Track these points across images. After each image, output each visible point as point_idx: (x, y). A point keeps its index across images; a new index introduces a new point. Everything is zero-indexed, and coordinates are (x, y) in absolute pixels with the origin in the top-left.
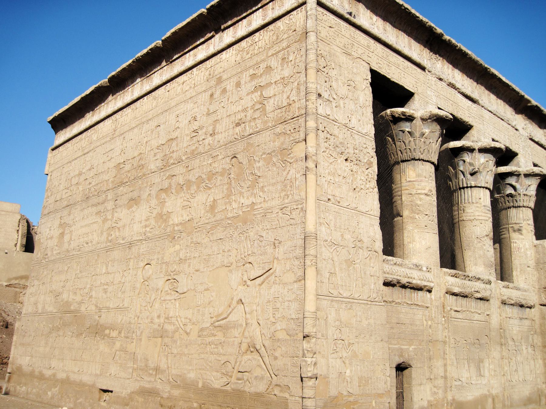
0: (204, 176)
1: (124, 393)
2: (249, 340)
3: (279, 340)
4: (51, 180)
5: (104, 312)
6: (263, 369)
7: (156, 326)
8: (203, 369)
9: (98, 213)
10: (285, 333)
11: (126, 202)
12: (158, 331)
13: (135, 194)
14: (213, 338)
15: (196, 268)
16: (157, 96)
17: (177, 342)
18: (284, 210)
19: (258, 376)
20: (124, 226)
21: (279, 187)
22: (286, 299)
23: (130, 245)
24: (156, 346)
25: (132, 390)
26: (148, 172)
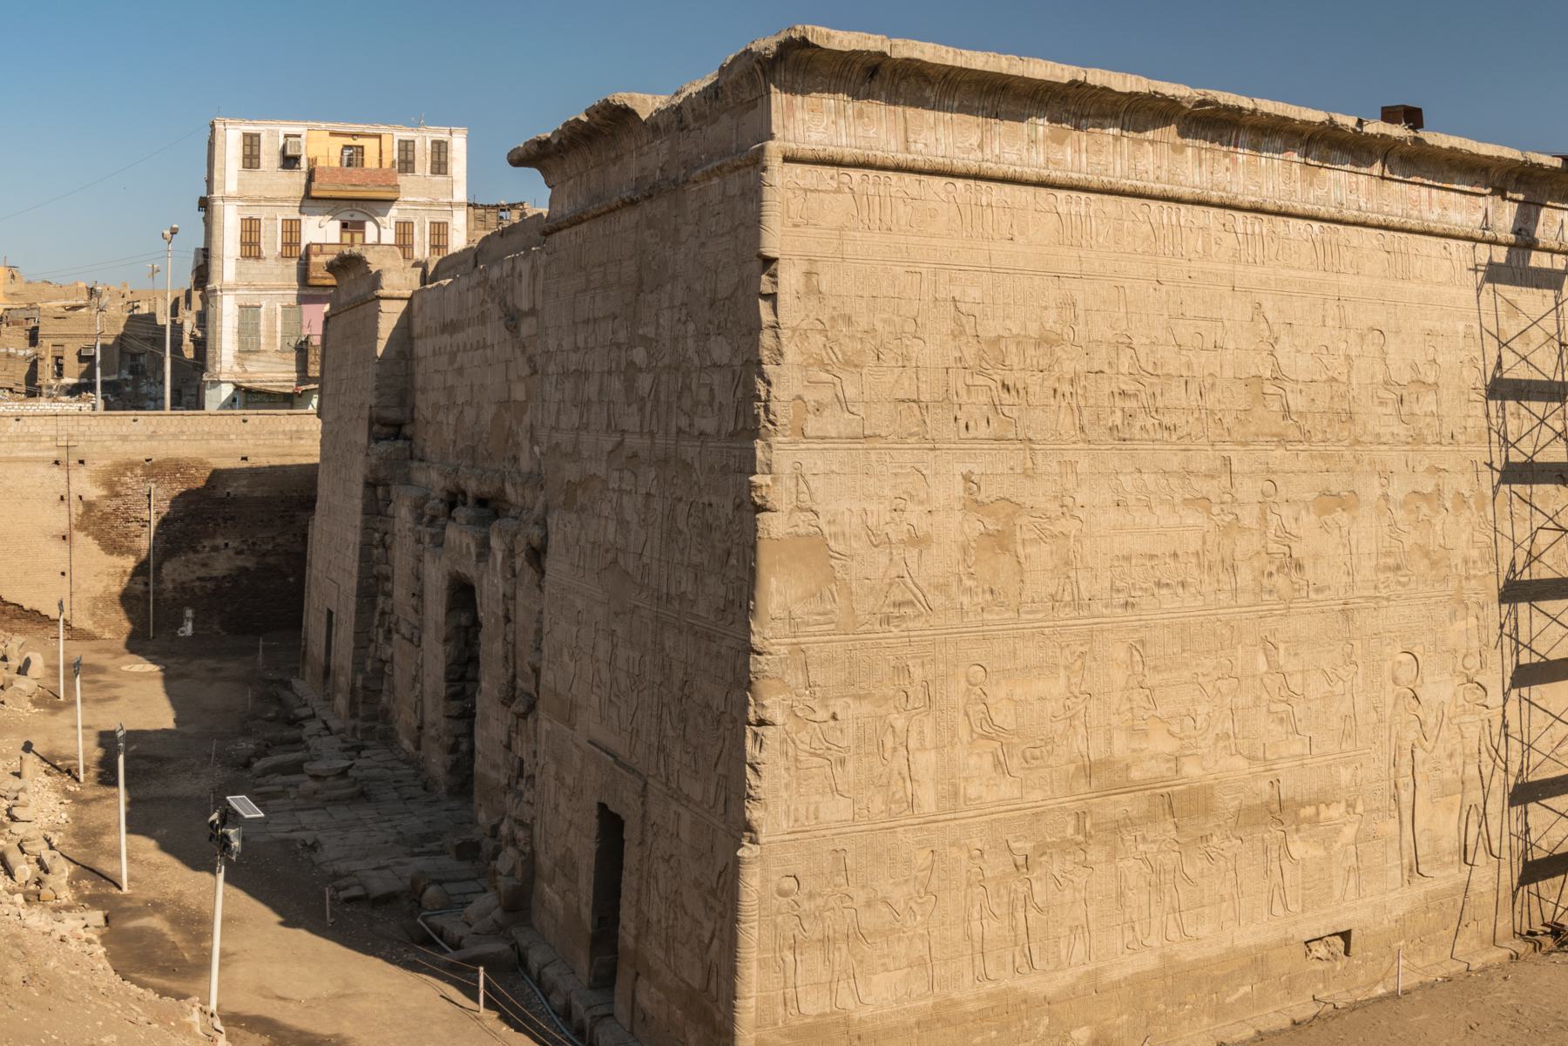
4: (811, 289)
9: (1202, 502)
11: (1310, 496)
13: (1337, 484)
16: (1355, 243)
20: (1316, 557)
26: (1370, 439)
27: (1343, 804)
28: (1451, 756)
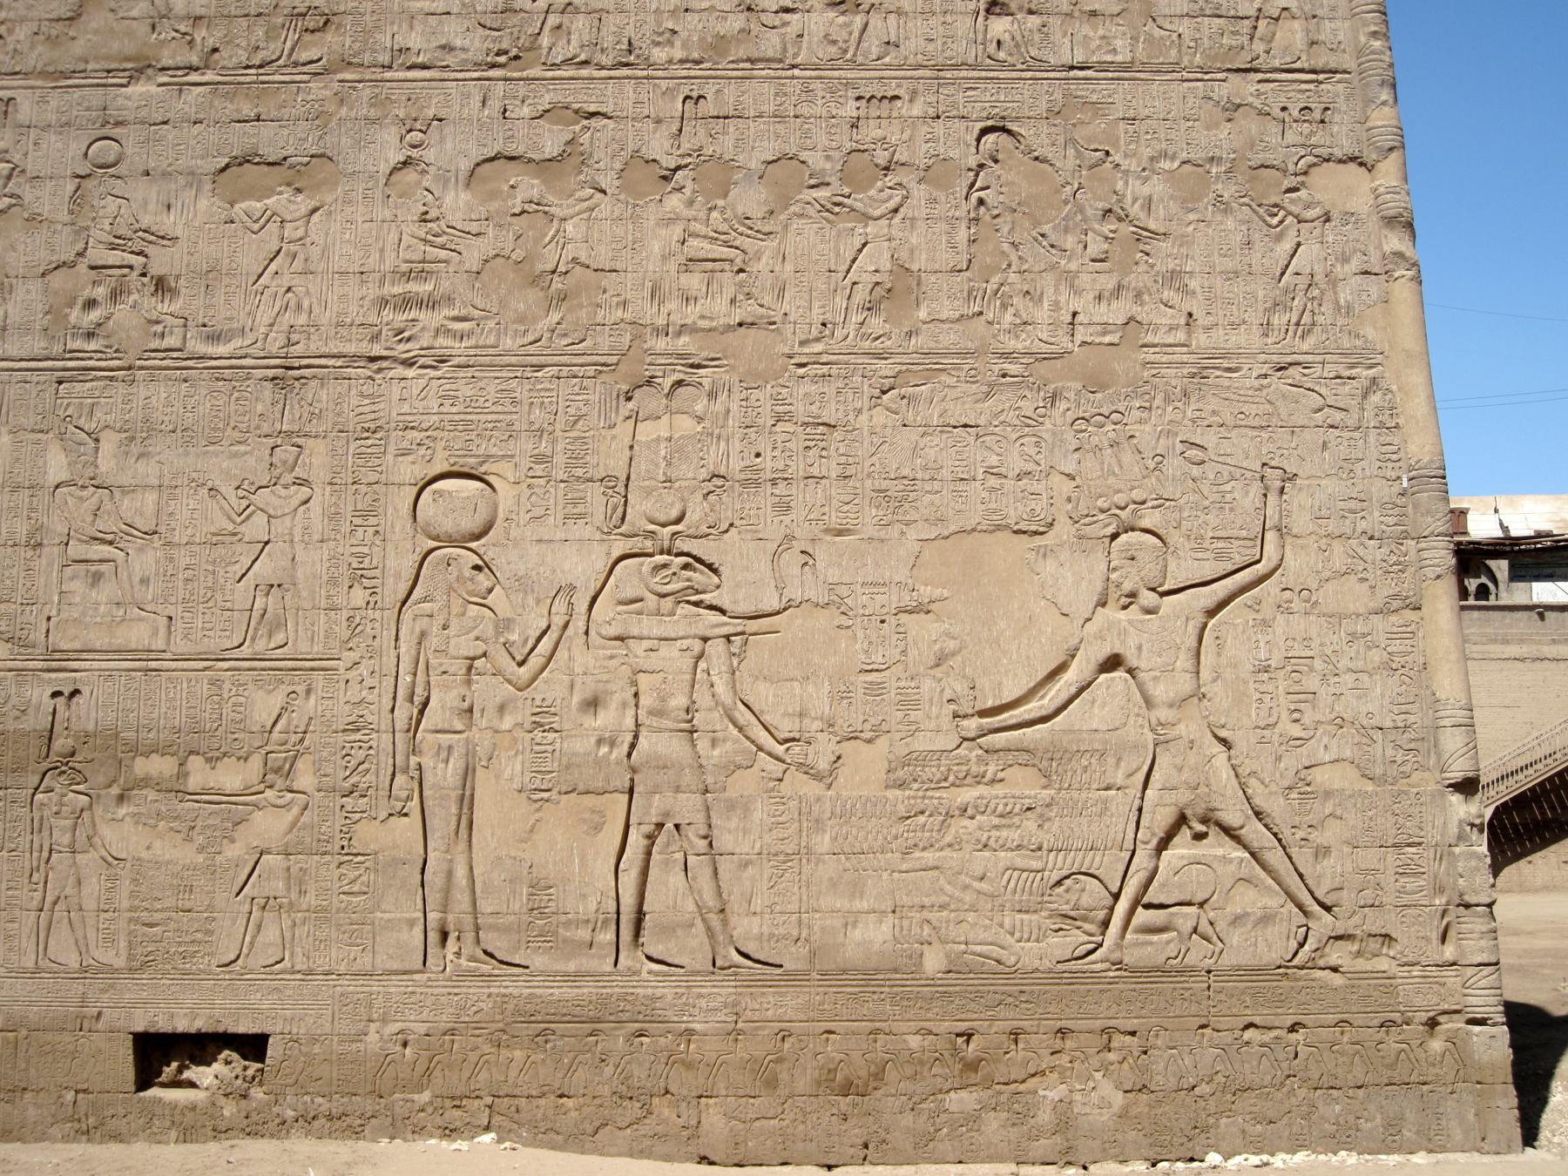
0: (815, 160)
1: (372, 1037)
2: (1183, 797)
3: (1328, 794)
5: (109, 675)
6: (1269, 888)
7: (581, 745)
8: (942, 907)
10: (1352, 773)
12: (599, 763)
14: (982, 790)
15: (834, 520)
17: (747, 810)
18: (1291, 371)
19: (1246, 914)
21: (1262, 291)
22: (1344, 663)
23: (287, 374)
24: (598, 828)
25: (445, 1020)
27: (256, 762)
28: (593, 704)
